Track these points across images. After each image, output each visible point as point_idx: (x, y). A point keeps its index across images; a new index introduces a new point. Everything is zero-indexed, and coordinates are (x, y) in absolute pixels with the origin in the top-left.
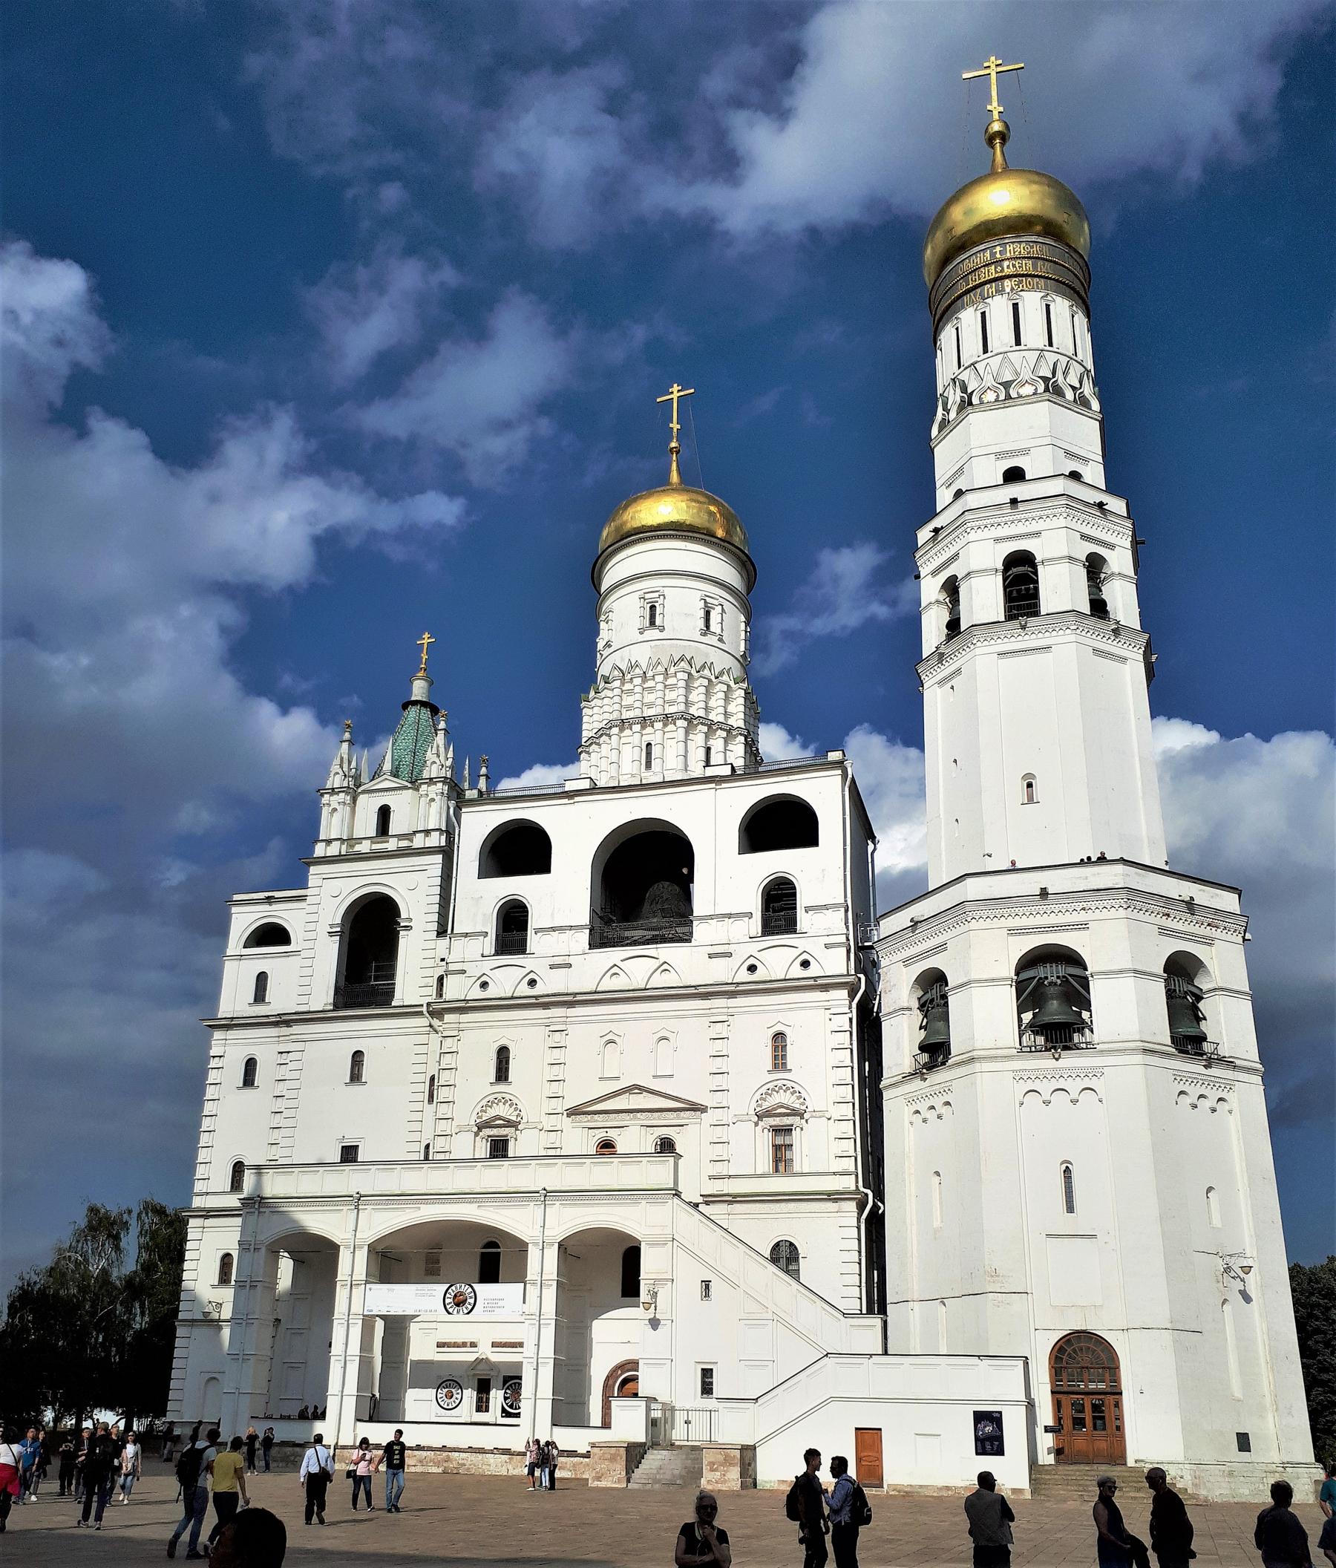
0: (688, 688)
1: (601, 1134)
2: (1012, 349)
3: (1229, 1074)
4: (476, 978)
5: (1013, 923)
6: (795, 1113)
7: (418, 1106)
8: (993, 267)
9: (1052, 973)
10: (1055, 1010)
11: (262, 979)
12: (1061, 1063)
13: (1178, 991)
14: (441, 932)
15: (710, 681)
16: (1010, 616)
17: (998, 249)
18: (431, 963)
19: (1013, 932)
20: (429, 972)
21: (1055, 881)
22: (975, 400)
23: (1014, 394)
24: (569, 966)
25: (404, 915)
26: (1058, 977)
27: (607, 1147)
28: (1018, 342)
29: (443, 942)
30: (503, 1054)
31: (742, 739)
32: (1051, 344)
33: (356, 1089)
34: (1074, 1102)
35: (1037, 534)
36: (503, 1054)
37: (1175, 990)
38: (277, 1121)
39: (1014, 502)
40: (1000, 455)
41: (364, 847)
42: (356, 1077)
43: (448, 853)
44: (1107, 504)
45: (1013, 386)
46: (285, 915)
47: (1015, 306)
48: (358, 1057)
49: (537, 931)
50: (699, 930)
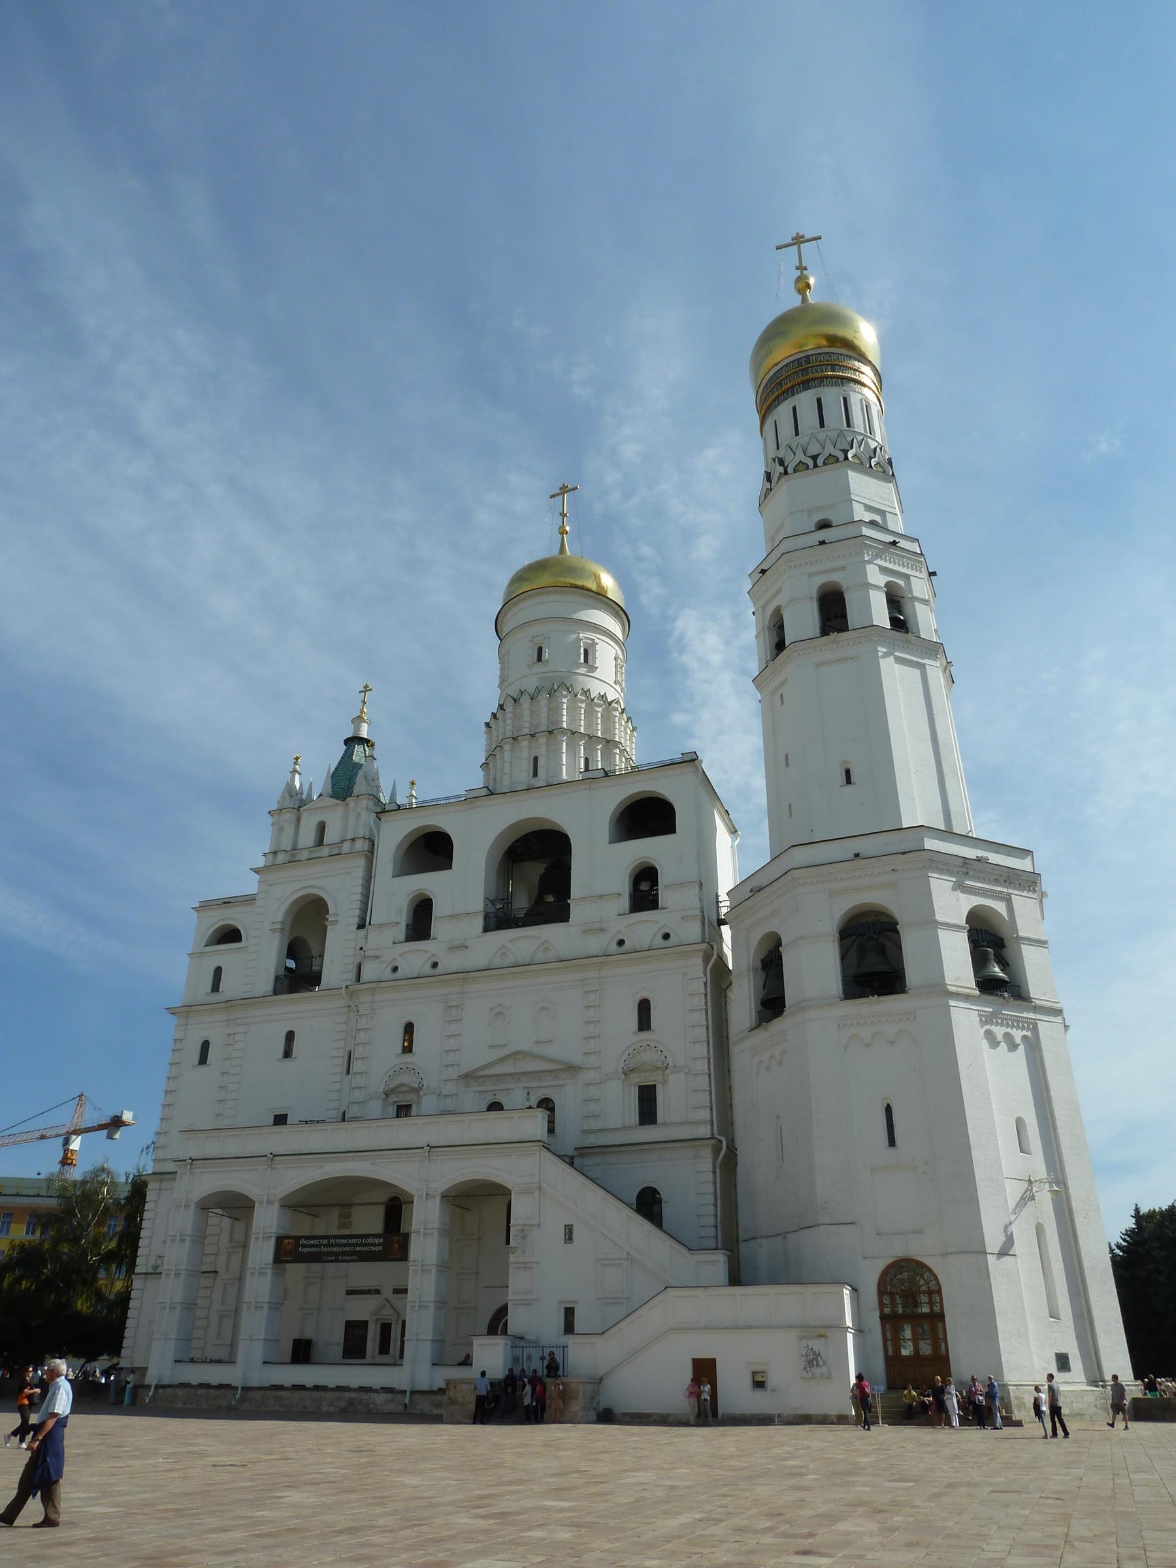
2: (817, 431)
3: (1032, 1015)
4: (386, 964)
8: (800, 373)
10: (874, 963)
11: (218, 971)
13: (981, 941)
14: (361, 926)
16: (825, 632)
17: (803, 360)
22: (790, 470)
23: (820, 462)
25: (331, 911)
26: (875, 932)
28: (822, 425)
29: (362, 932)
30: (409, 1029)
32: (849, 425)
34: (892, 1043)
35: (843, 568)
36: (409, 1029)
37: (979, 940)
39: (822, 543)
40: (810, 512)
44: (897, 543)
45: (819, 457)
47: (819, 401)
48: (290, 1036)
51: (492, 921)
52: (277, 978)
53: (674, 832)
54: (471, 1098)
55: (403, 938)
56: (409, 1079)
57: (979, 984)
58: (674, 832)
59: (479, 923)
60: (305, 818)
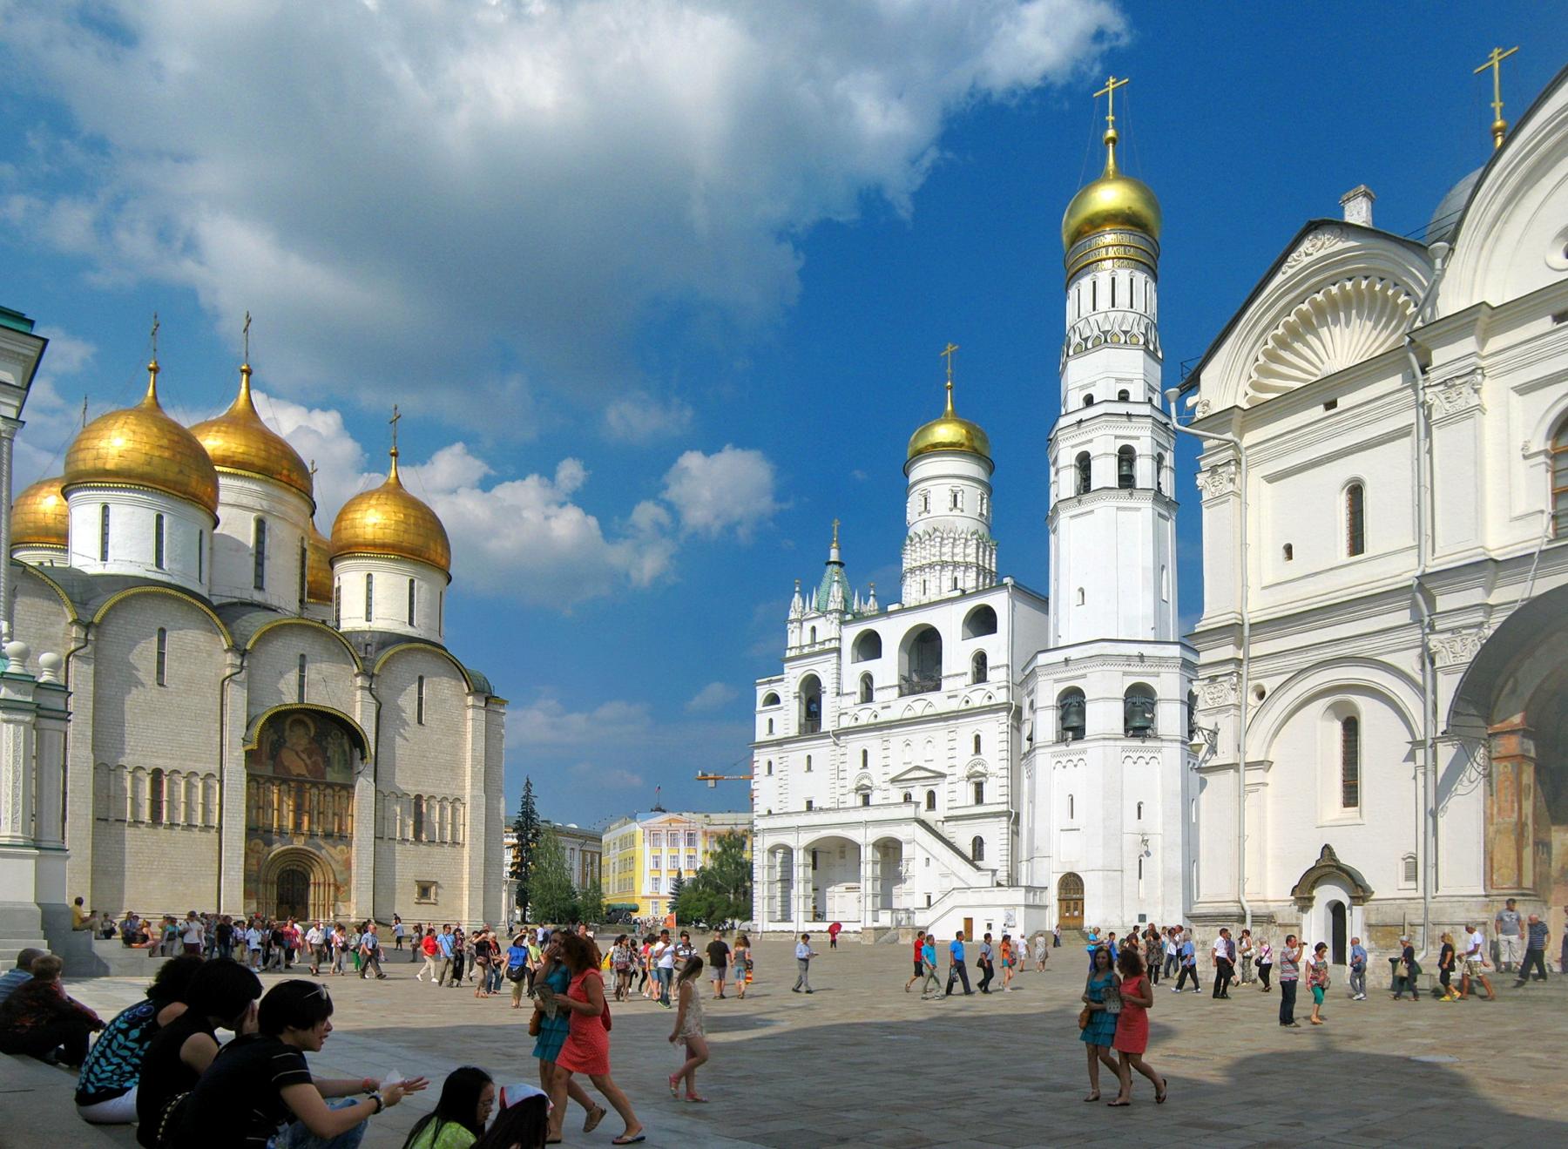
0: (941, 545)
1: (905, 790)
5: (1055, 677)
6: (984, 775)
7: (833, 781)
9: (1073, 700)
10: (1074, 721)
11: (771, 721)
12: (1070, 747)
14: (838, 694)
15: (954, 539)
18: (834, 709)
19: (1057, 681)
20: (834, 714)
21: (1073, 653)
24: (889, 707)
27: (907, 798)
29: (839, 698)
30: (865, 752)
31: (974, 569)
33: (809, 773)
36: (865, 752)
38: (781, 791)
41: (806, 651)
42: (809, 769)
43: (838, 650)
46: (778, 689)
48: (809, 757)
49: (877, 689)
50: (944, 683)
51: (906, 691)
52: (800, 725)
53: (995, 631)
54: (896, 795)
55: (858, 701)
56: (866, 782)
57: (1126, 731)
58: (995, 631)
59: (896, 691)
60: (804, 623)
